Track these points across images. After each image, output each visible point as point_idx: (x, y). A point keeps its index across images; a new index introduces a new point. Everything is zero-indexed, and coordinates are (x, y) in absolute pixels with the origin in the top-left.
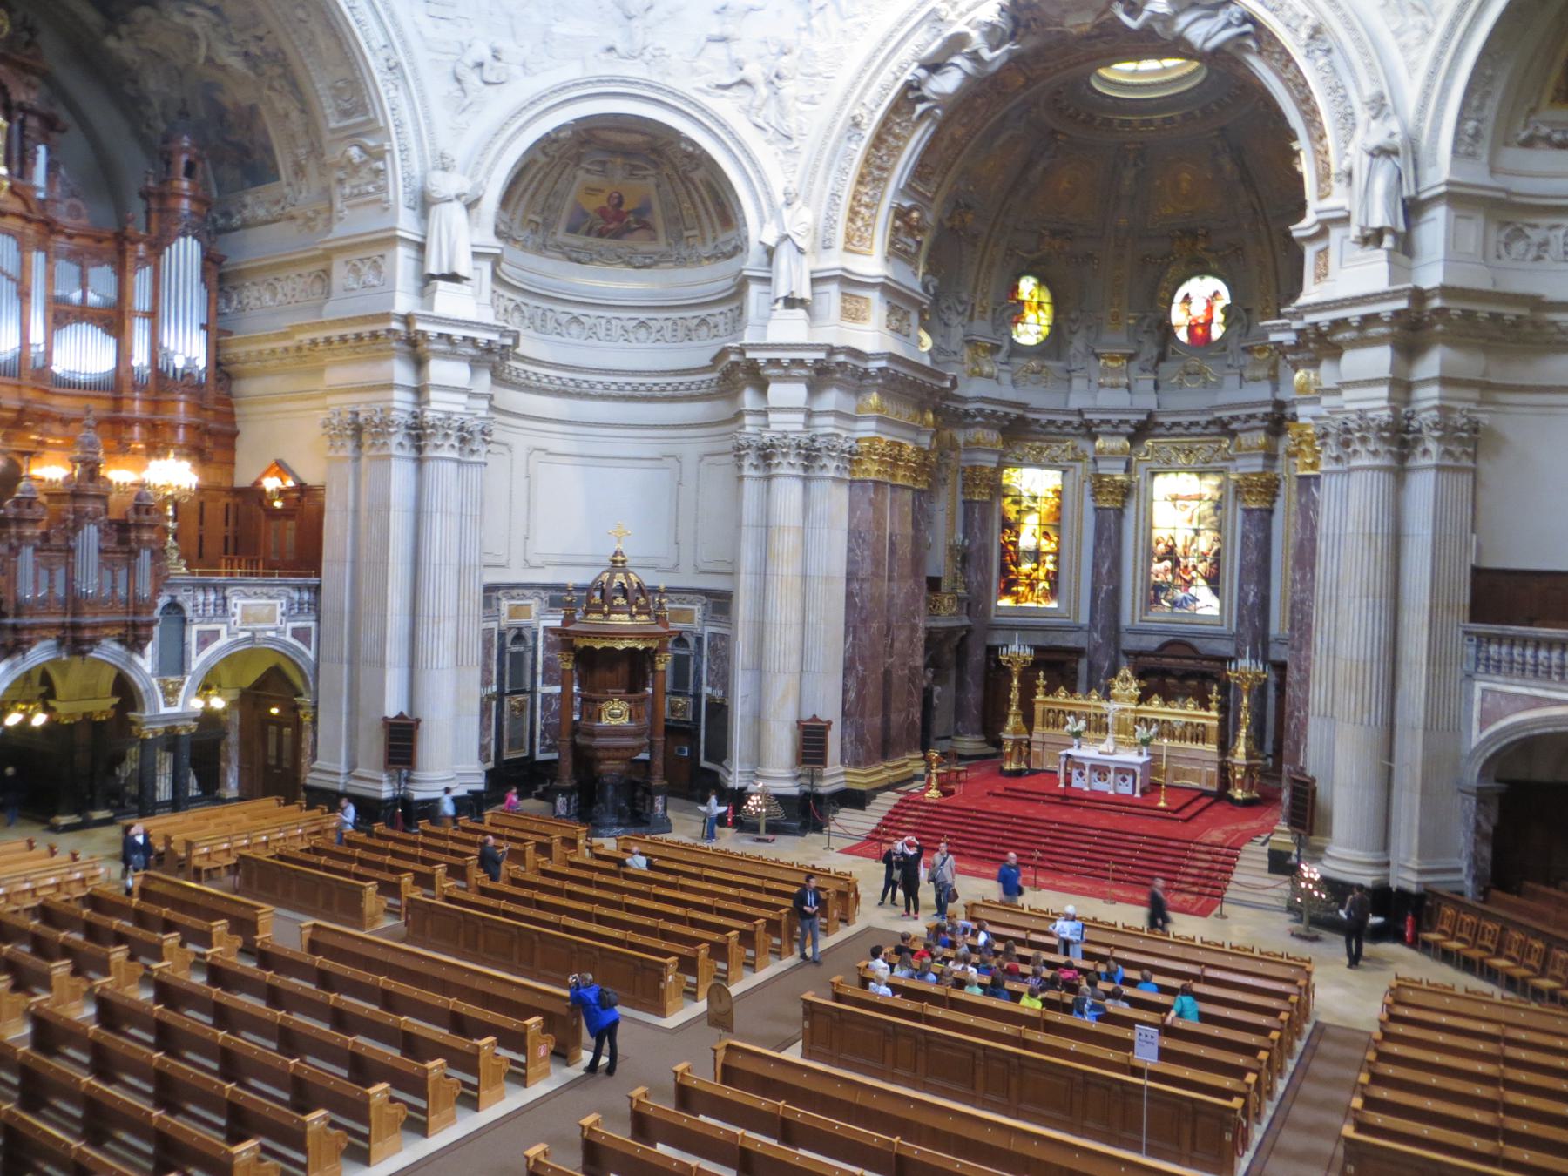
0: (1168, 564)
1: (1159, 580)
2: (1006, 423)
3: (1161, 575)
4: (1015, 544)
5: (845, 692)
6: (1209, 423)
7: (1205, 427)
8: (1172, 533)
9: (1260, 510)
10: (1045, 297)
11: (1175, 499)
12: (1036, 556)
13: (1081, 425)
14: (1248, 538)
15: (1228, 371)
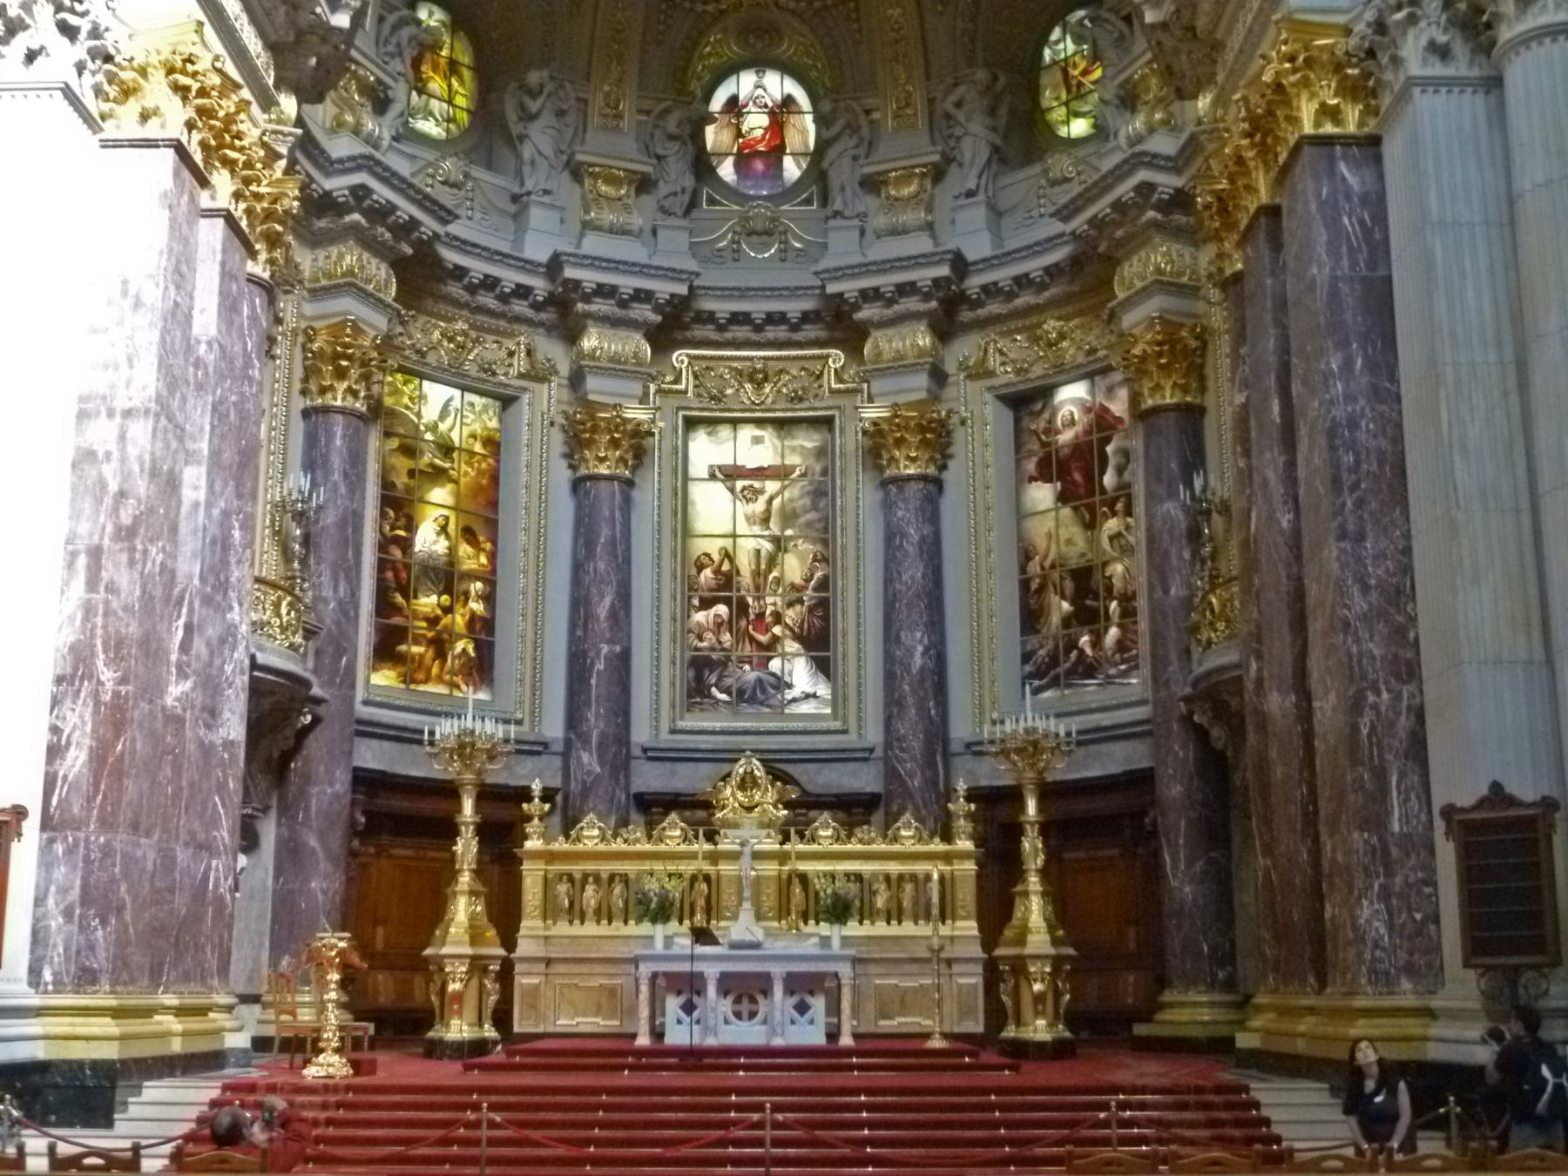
0: (722, 609)
1: (705, 644)
2: (409, 251)
3: (709, 635)
4: (406, 545)
5: (54, 752)
6: (806, 317)
7: (795, 328)
8: (728, 543)
9: (923, 478)
10: (465, 58)
11: (729, 474)
12: (446, 577)
13: (551, 300)
14: (903, 535)
15: (832, 223)
